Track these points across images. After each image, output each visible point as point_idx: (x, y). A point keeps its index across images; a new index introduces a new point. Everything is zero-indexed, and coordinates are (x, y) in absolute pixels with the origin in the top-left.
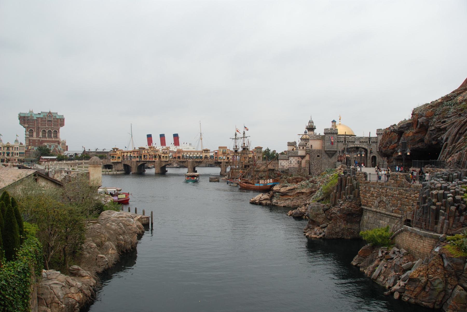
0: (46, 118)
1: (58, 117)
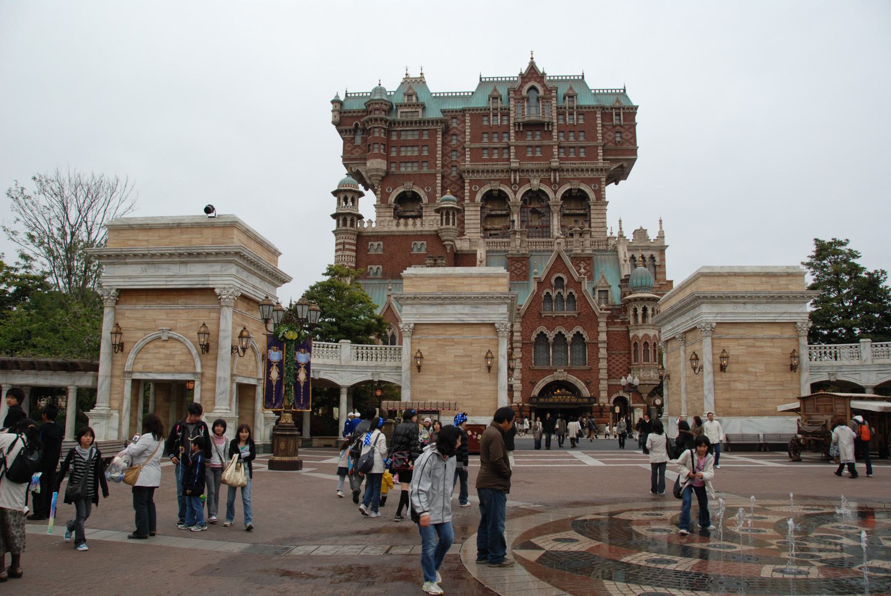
0: (506, 113)
1: (585, 101)
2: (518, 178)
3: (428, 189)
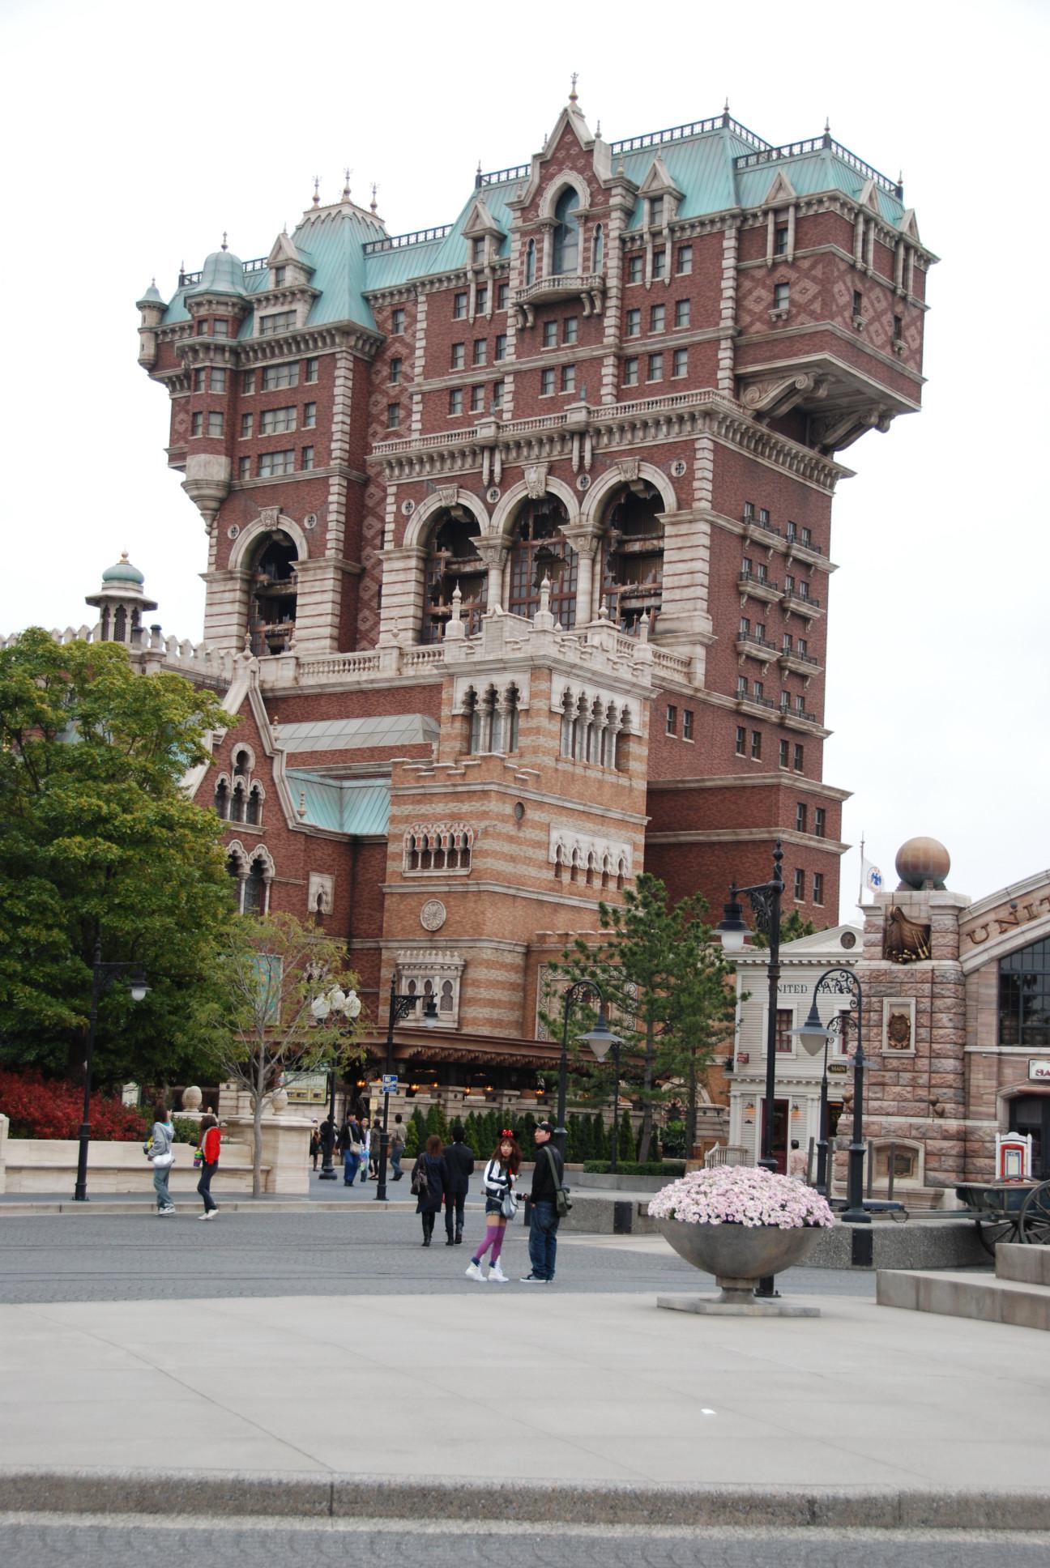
2: (497, 469)
3: (311, 520)
